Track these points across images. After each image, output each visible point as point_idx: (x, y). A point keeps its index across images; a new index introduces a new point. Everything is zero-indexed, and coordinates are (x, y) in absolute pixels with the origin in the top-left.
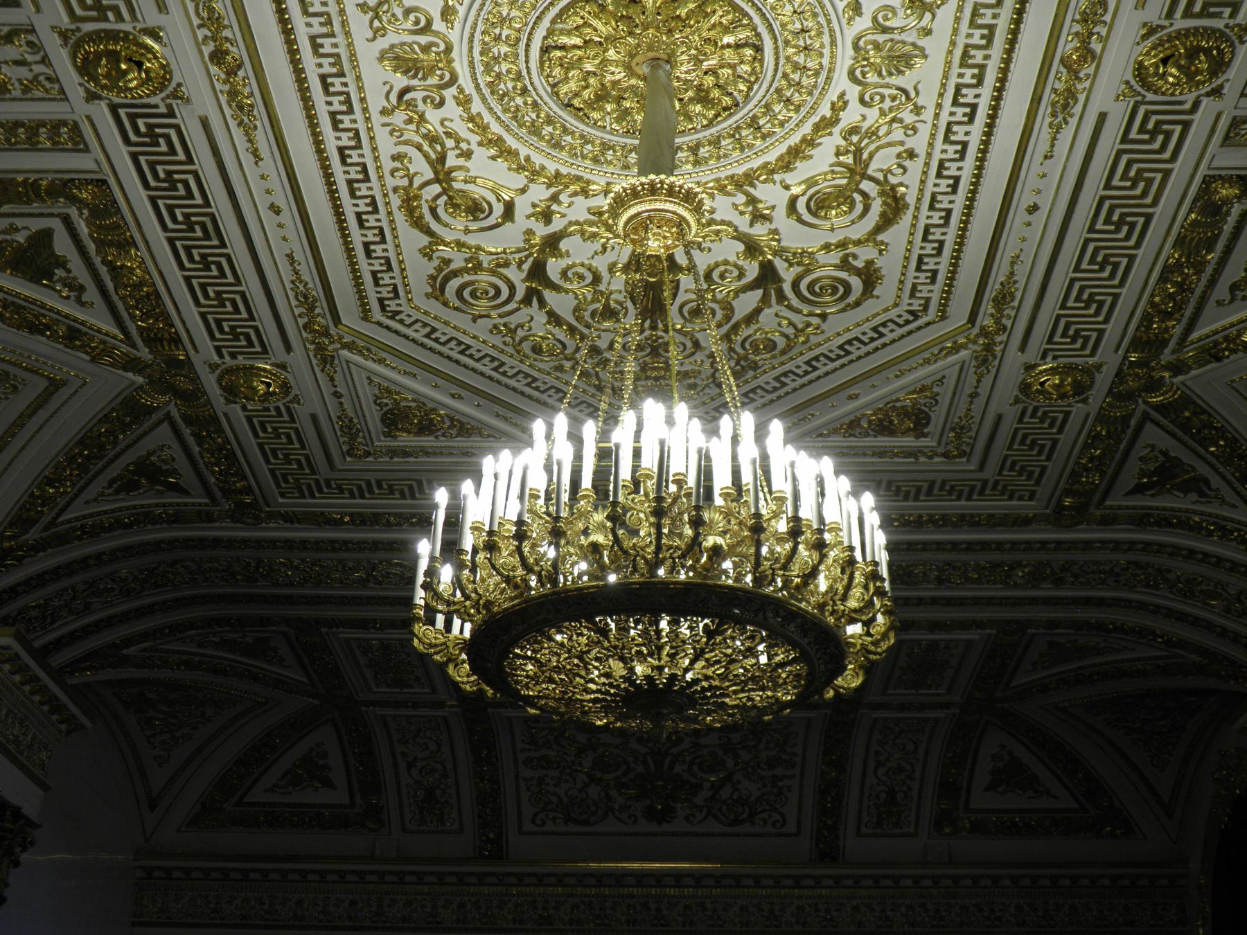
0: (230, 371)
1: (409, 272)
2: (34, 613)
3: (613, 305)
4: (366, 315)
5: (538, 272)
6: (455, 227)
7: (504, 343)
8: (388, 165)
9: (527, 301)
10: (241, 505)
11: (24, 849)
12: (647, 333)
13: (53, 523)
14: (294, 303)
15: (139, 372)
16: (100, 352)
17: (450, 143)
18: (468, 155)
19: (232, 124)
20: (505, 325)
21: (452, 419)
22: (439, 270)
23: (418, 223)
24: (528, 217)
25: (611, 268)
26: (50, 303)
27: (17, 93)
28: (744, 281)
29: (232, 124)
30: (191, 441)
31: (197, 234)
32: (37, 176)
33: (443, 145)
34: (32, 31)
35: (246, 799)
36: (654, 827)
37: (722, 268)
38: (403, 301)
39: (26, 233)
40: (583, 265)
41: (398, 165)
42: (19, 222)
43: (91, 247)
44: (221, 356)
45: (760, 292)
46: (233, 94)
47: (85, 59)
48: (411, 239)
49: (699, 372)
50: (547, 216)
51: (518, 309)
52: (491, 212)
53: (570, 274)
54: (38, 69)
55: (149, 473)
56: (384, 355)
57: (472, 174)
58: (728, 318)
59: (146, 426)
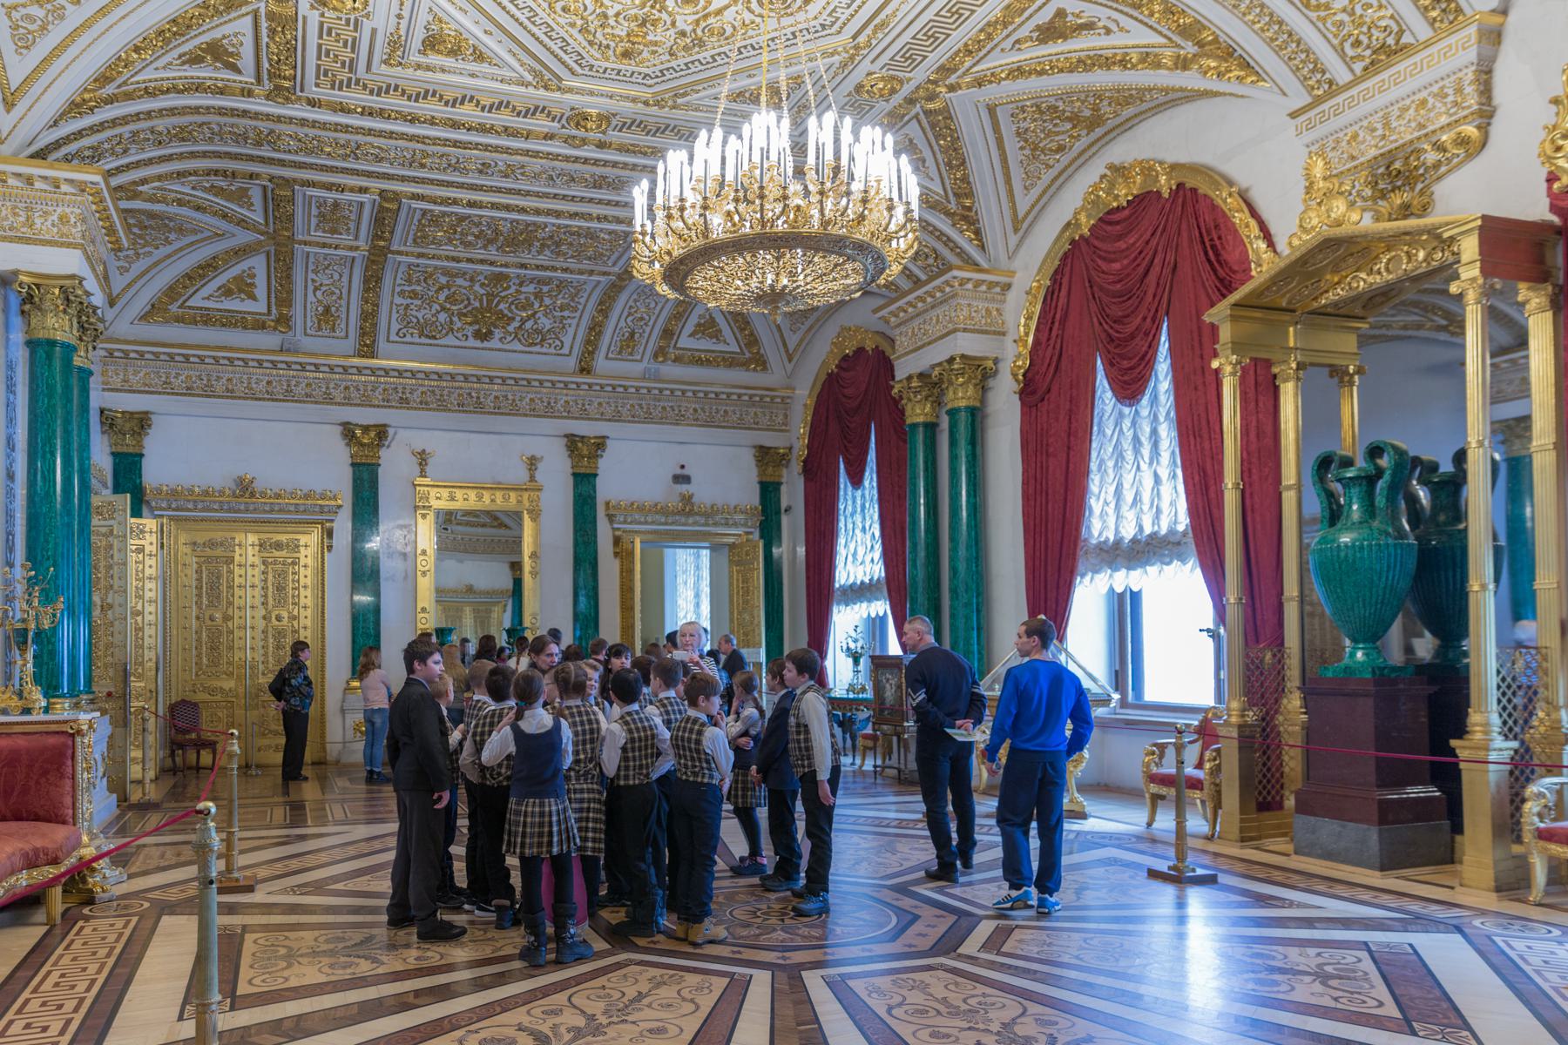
2: (87, 153)
10: (278, 88)
13: (125, 83)
21: (475, 48)
30: (264, 32)
36: (478, 344)
55: (217, 52)
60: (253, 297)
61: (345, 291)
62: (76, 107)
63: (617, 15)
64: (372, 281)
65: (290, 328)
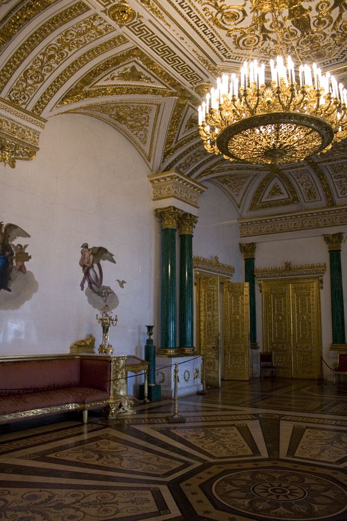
0: (196, 88)
1: (227, 43)
3: (291, 31)
4: (222, 60)
5: (263, 29)
6: (231, 25)
7: (265, 55)
8: (203, 13)
9: (265, 39)
11: (196, 223)
12: (307, 36)
13: (177, 141)
14: (202, 63)
15: (176, 96)
16: (163, 94)
19: (157, 18)
20: (262, 49)
22: (234, 39)
23: (221, 27)
24: (251, 13)
25: (284, 19)
26: (145, 85)
27: (105, 33)
28: (330, 6)
29: (157, 18)
31: (166, 53)
32: (122, 53)
34: (98, 15)
35: (262, 201)
37: (321, 5)
38: (229, 52)
39: (129, 69)
41: (205, 12)
42: (126, 66)
43: (145, 67)
44: (192, 85)
45: (338, 8)
46: (152, 10)
47: (113, 16)
48: (222, 33)
49: (330, 43)
51: (263, 43)
52: (239, 16)
53: (273, 26)
54: (105, 24)
56: (234, 70)
57: (228, 5)
58: (331, 21)
59: (185, 110)
60: (281, 193)
61: (313, 182)
62: (166, 154)
64: (321, 175)
65: (298, 201)
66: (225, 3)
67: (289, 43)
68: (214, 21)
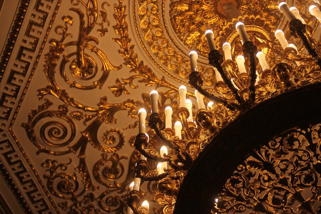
1: (23, 105)
5: (93, 128)
9: (76, 147)
17: (100, 20)
18: (103, 31)
22: (41, 108)
33: (95, 20)
40: (118, 132)
48: (40, 79)
50: (121, 90)
63: (102, 196)
66: (100, 39)
67: (95, 183)
68: (52, 50)
